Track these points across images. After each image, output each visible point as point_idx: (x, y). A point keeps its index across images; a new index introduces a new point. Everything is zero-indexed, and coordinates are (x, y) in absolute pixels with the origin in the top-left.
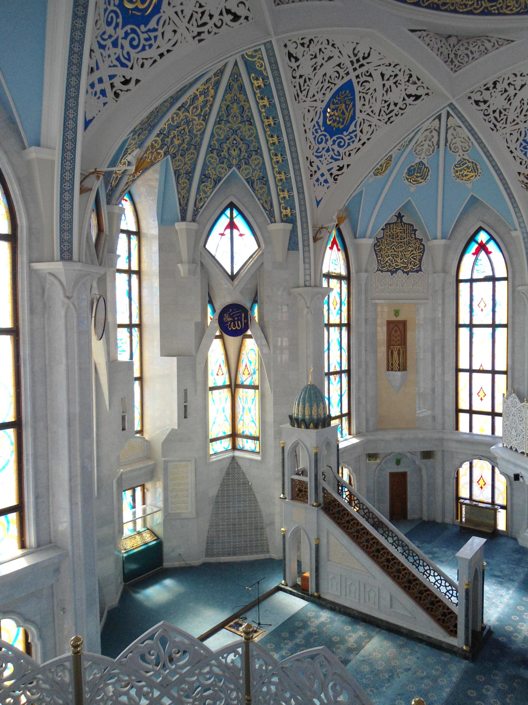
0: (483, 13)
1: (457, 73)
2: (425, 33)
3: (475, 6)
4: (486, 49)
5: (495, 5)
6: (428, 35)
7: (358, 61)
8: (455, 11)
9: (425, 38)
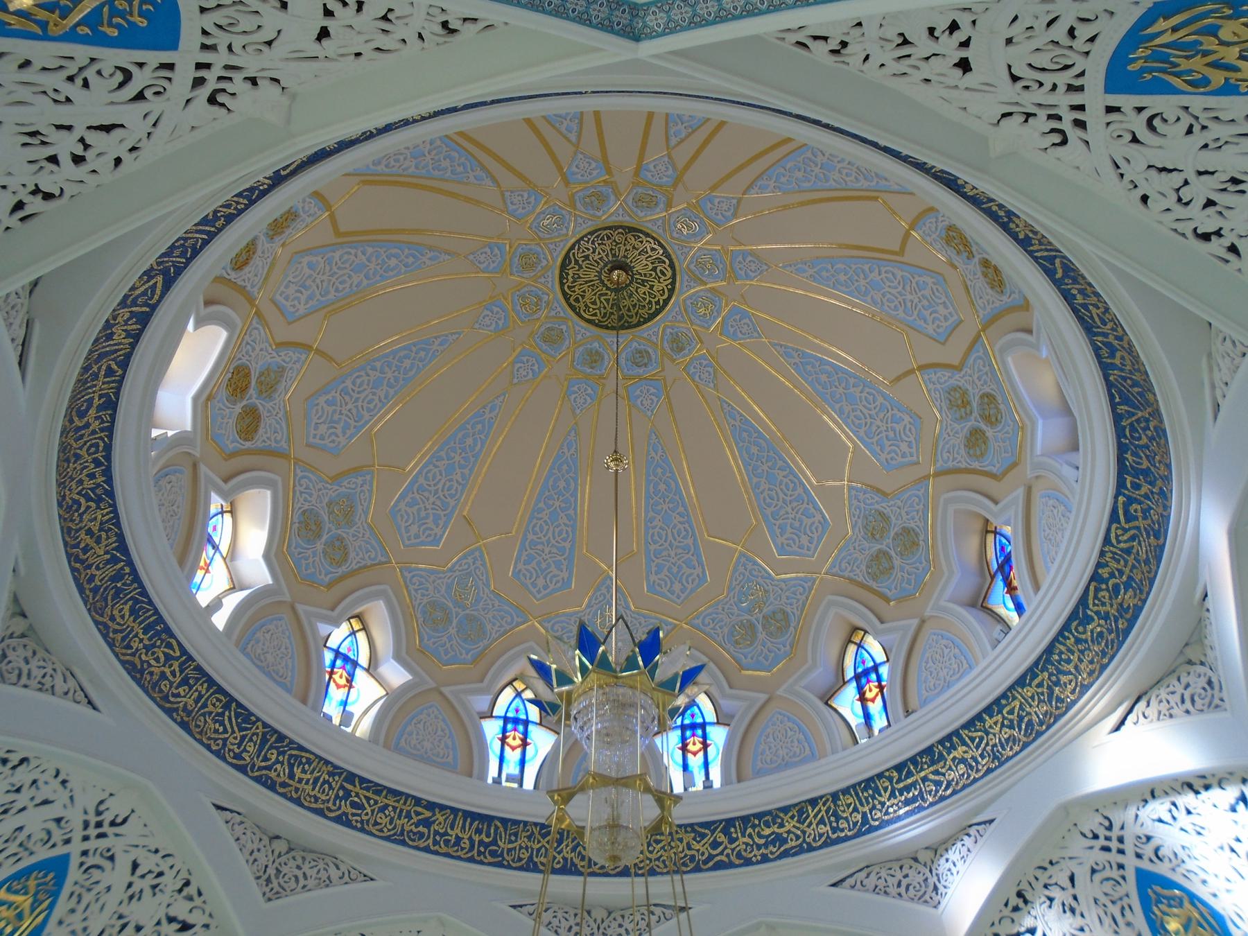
0: (338, 820)
1: (271, 903)
2: (238, 818)
3: (330, 805)
4: (329, 878)
5: (359, 815)
6: (242, 823)
7: (99, 825)
8: (298, 802)
9: (236, 827)
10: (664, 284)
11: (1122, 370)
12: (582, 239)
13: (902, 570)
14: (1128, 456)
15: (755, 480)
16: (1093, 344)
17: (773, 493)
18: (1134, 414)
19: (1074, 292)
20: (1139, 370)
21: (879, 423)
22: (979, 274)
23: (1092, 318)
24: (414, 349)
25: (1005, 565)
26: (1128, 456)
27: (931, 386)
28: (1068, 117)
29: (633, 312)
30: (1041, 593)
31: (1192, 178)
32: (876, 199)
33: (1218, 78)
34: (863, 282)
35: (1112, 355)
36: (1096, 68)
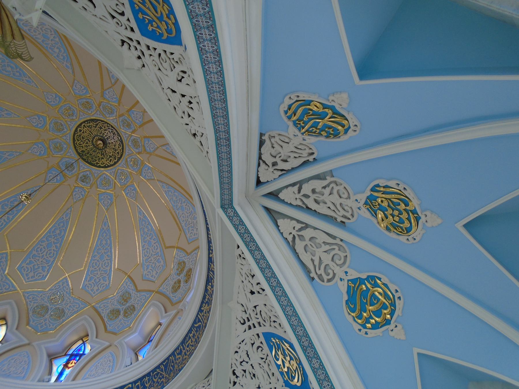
10: (107, 163)
11: (175, 360)
12: (108, 123)
13: (45, 320)
14: (147, 378)
15: (45, 239)
16: (179, 346)
17: (43, 250)
18: (162, 371)
19: (193, 332)
20: (179, 366)
21: (99, 273)
22: (174, 281)
23: (187, 342)
24: (18, 70)
25: (73, 356)
26: (147, 378)
27: (125, 284)
28: (250, 323)
29: (88, 155)
30: (74, 382)
31: (250, 363)
32: (180, 230)
33: (280, 362)
34: (148, 238)
35: (178, 354)
36: (267, 329)
